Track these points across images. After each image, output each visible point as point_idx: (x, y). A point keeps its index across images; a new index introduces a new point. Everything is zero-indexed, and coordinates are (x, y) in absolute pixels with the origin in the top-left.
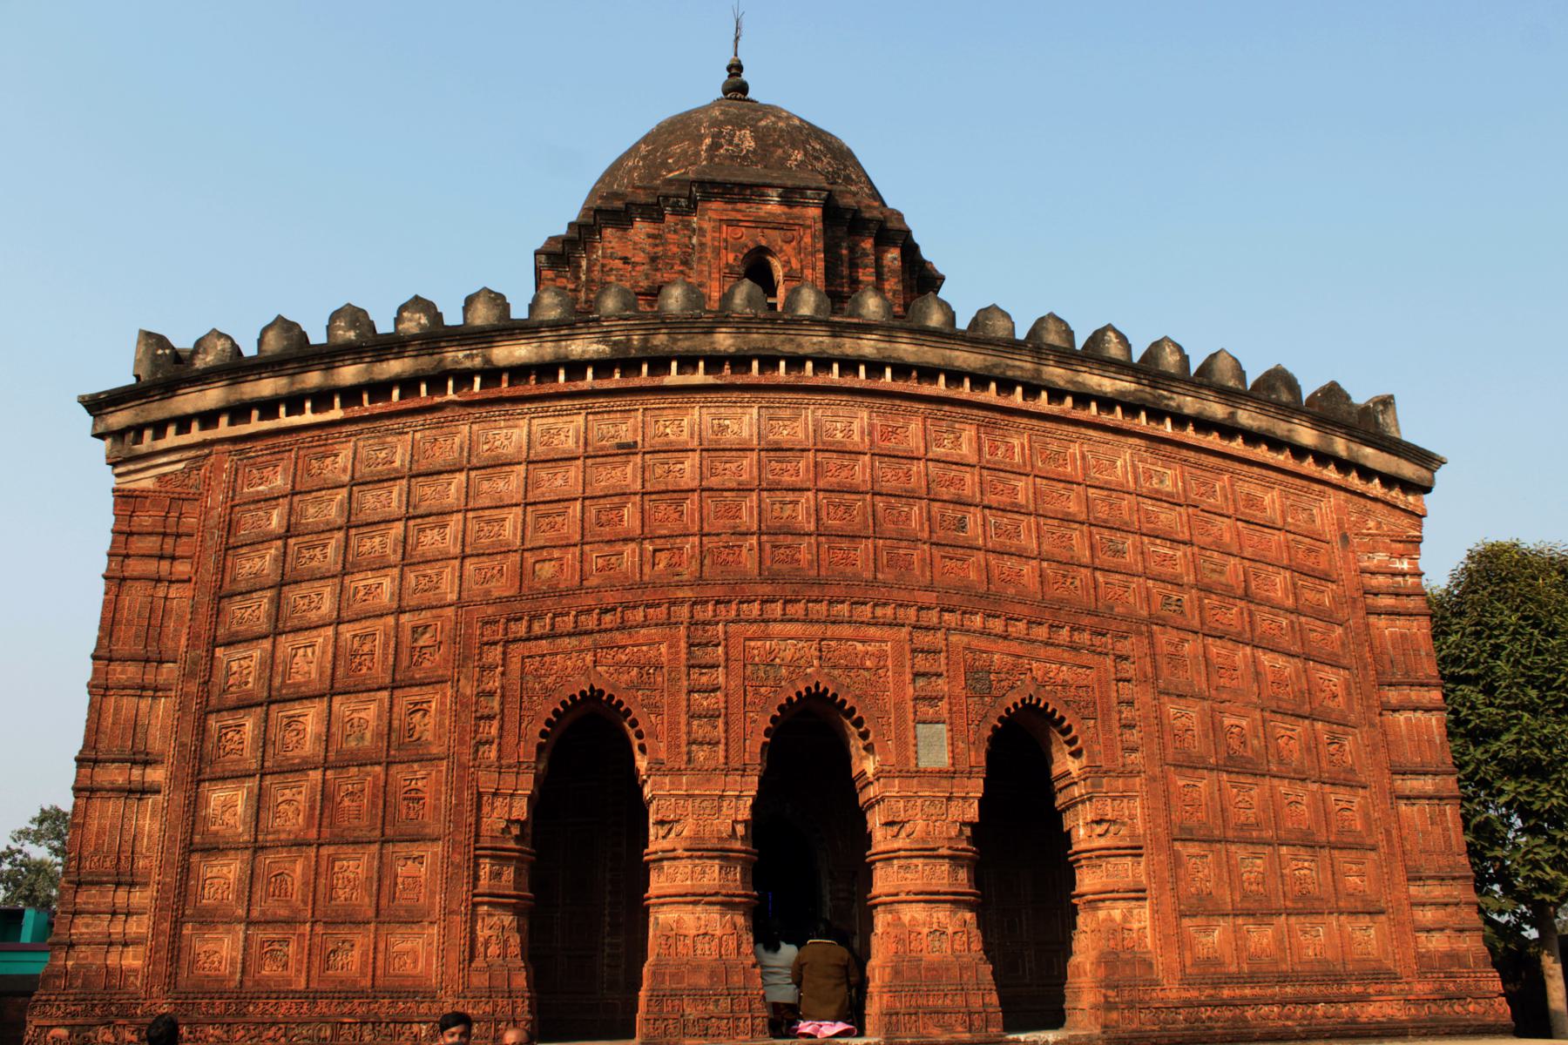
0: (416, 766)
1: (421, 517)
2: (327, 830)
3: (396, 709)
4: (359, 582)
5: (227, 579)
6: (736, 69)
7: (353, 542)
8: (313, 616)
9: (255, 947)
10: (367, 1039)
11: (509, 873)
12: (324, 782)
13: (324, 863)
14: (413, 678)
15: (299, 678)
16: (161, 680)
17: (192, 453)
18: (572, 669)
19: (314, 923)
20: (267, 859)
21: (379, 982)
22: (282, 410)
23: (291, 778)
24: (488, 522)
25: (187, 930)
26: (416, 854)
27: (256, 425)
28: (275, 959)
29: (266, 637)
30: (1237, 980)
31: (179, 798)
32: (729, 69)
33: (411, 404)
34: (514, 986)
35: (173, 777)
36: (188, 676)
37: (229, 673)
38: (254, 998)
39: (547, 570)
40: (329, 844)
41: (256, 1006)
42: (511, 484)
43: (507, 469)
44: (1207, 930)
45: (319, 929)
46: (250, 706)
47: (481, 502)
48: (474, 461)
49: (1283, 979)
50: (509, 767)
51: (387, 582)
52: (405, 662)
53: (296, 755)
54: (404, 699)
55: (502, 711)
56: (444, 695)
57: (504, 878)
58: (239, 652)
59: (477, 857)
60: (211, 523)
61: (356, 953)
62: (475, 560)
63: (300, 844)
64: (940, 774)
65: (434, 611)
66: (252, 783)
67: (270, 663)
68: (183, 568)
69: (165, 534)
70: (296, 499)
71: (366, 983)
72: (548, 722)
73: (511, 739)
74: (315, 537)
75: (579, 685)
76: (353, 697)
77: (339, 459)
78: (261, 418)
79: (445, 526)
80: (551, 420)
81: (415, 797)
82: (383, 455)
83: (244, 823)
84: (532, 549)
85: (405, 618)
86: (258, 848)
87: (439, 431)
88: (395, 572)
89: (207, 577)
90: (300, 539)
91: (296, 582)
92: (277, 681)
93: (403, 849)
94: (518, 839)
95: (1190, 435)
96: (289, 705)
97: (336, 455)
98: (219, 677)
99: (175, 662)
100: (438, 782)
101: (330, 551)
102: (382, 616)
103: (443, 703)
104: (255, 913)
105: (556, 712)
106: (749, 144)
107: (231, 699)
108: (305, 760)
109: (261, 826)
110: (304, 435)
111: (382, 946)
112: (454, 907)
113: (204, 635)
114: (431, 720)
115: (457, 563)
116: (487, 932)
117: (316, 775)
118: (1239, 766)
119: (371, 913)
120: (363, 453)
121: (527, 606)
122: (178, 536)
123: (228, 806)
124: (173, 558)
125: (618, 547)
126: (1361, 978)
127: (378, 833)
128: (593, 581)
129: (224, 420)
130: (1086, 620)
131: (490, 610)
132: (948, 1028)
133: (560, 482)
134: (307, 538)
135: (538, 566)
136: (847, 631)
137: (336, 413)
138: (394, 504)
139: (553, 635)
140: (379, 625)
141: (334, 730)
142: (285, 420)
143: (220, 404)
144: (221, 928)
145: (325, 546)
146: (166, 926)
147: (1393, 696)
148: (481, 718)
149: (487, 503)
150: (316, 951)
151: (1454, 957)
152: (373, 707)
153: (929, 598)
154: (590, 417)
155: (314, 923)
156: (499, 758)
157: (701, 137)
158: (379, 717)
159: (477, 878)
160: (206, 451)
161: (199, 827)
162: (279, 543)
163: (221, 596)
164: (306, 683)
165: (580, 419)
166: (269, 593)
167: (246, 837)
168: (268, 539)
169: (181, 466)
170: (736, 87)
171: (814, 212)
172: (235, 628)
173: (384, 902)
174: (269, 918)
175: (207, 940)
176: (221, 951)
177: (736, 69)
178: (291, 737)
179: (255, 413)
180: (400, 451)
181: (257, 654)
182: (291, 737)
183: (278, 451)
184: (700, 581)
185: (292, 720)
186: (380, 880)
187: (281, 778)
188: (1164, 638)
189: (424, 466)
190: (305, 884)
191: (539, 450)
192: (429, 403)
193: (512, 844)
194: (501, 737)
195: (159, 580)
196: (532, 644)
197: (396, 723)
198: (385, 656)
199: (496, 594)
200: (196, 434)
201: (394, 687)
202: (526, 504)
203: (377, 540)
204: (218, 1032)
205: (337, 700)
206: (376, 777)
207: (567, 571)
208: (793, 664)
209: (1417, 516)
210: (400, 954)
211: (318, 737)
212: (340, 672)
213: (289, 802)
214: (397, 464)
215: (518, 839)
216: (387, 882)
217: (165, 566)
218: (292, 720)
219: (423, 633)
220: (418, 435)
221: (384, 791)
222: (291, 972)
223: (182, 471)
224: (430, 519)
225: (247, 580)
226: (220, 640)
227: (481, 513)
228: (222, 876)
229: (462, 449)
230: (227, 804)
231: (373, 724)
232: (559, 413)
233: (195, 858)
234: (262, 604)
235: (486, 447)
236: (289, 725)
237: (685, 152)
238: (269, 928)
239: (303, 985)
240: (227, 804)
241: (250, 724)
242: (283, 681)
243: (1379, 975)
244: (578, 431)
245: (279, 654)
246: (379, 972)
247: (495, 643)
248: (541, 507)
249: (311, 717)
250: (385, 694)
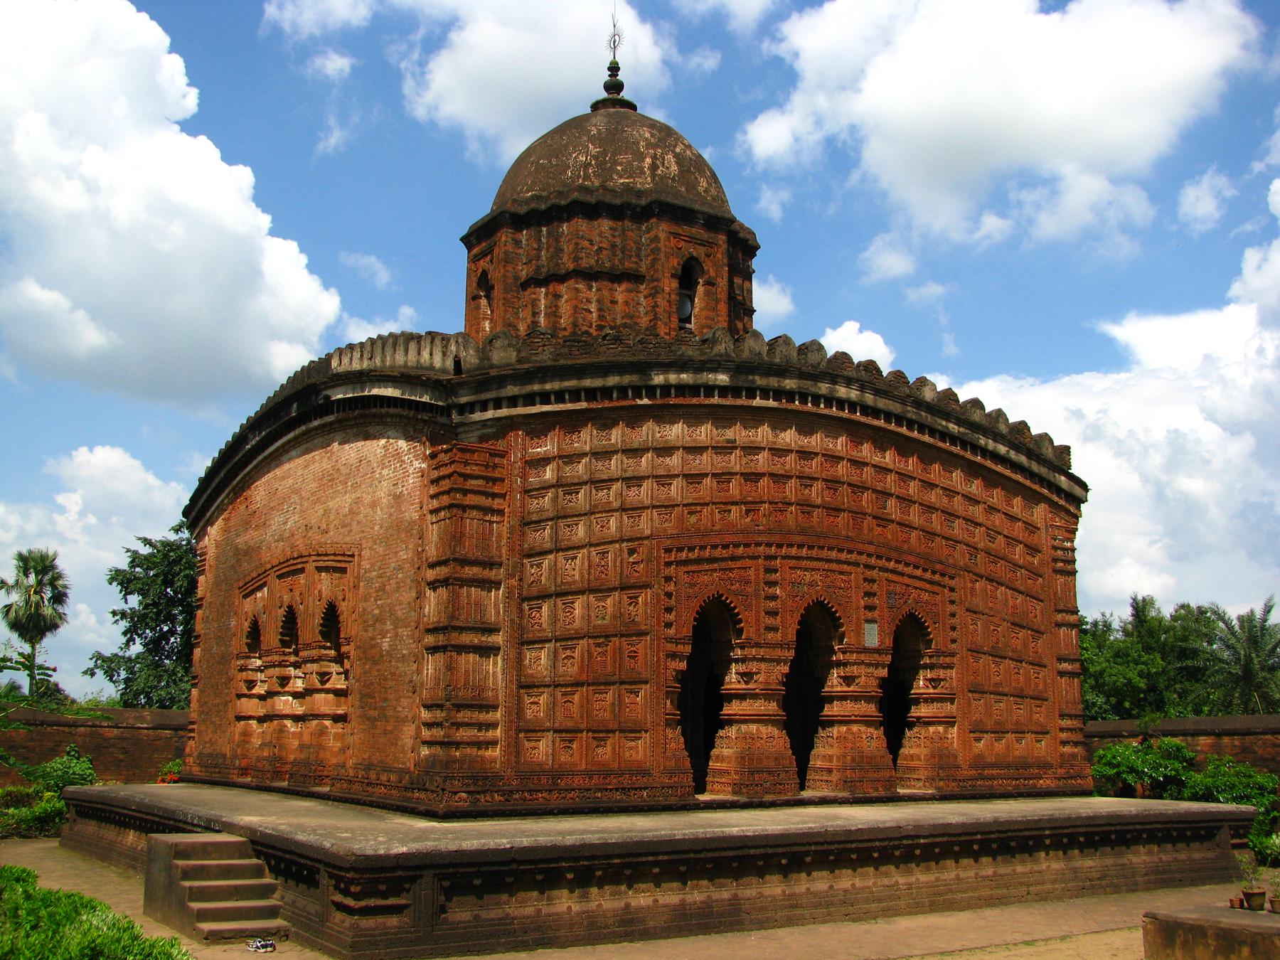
6: (614, 69)
18: (710, 582)
30: (992, 766)
32: (609, 69)
42: (675, 461)
44: (978, 740)
49: (1008, 767)
51: (613, 523)
64: (875, 651)
67: (554, 568)
75: (712, 591)
78: (542, 403)
85: (625, 544)
95: (989, 464)
106: (674, 168)
107: (534, 591)
108: (576, 630)
118: (998, 655)
125: (729, 507)
126: (1039, 767)
128: (718, 527)
130: (938, 567)
131: (668, 542)
132: (877, 789)
136: (834, 566)
140: (611, 548)
146: (513, 733)
147: (1059, 617)
151: (1073, 756)
153: (871, 549)
157: (641, 157)
164: (575, 582)
168: (546, 487)
170: (614, 86)
171: (722, 238)
176: (542, 749)
177: (614, 69)
179: (538, 399)
184: (769, 532)
188: (968, 576)
198: (615, 566)
208: (811, 584)
209: (1076, 517)
211: (583, 617)
231: (610, 610)
237: (630, 163)
243: (1046, 766)
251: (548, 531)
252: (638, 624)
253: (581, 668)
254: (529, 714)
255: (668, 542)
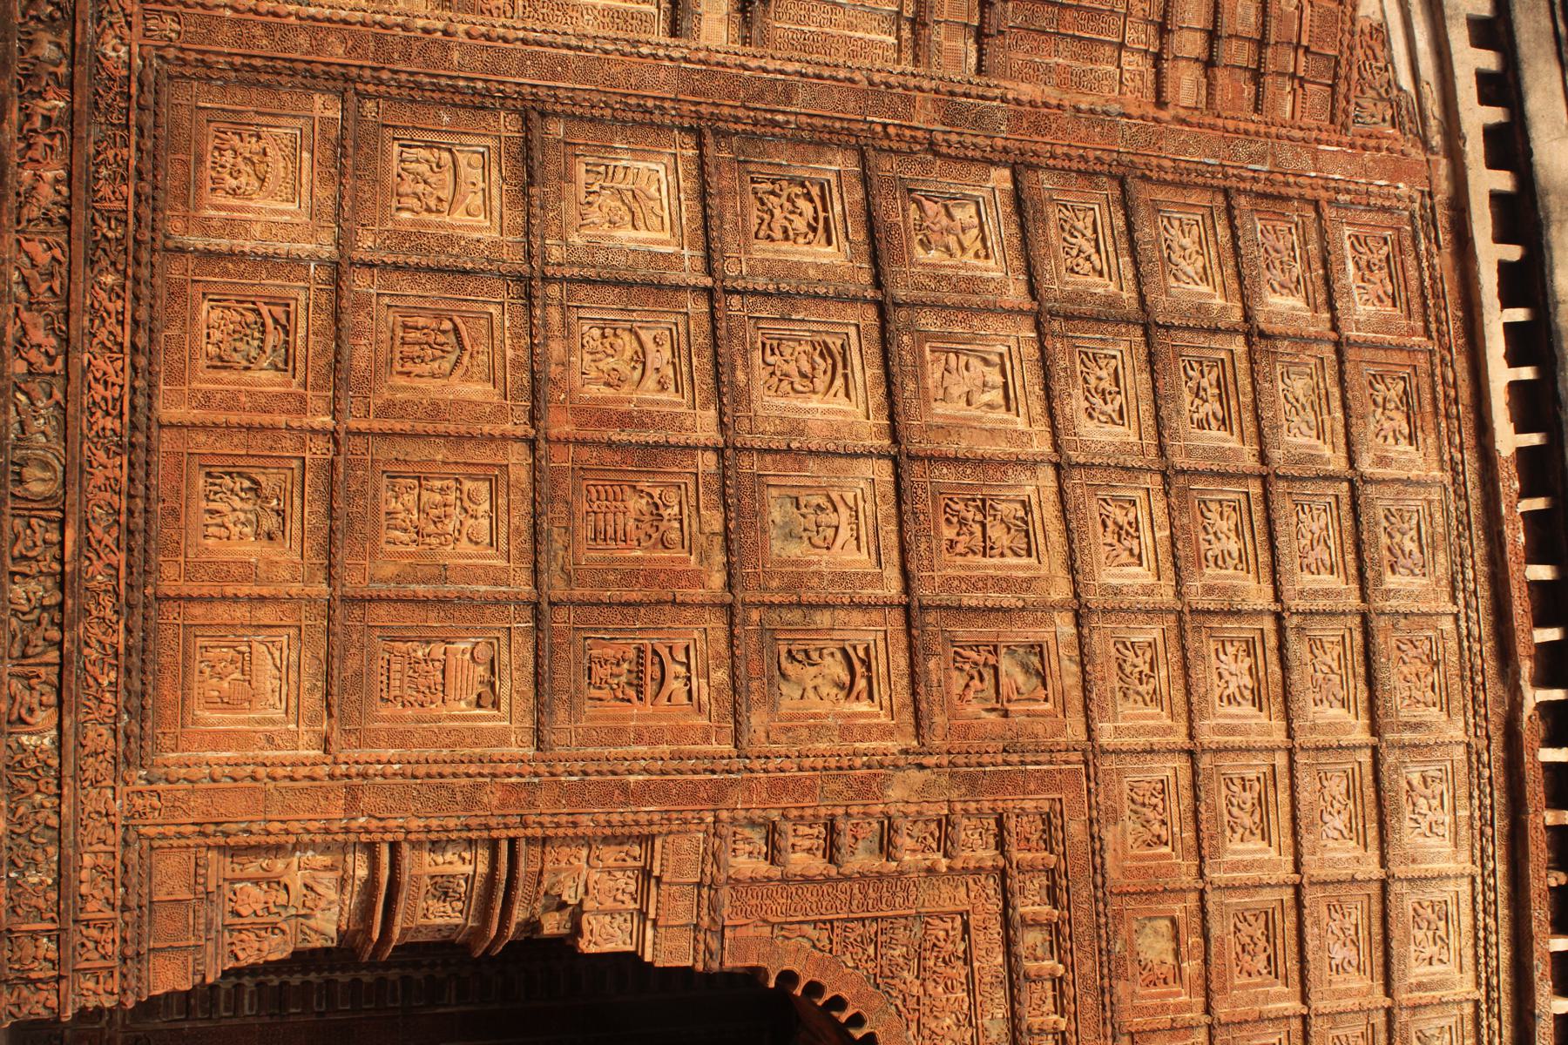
0: (720, 675)
1: (1282, 647)
2: (564, 460)
3: (857, 617)
4: (1145, 504)
5: (1161, 195)
7: (1232, 492)
8: (1074, 404)
9: (273, 284)
10: (18, 591)
11: (445, 916)
12: (689, 449)
13: (484, 455)
14: (929, 653)
15: (934, 373)
16: (939, 35)
17: (1433, 107)
19: (333, 435)
20: (497, 308)
21: (171, 612)
22: (1519, 315)
23: (701, 363)
24: (1261, 801)
25: (325, 107)
26: (504, 691)
27: (1491, 255)
28: (239, 334)
29: (1033, 291)
31: (660, 85)
33: (1520, 607)
34: (157, 962)
35: (711, 67)
36: (950, 104)
37: (949, 202)
38: (136, 287)
39: (1154, 946)
40: (535, 468)
41: (115, 293)
42: (1340, 851)
43: (1372, 833)
45: (318, 450)
46: (875, 259)
47: (1305, 780)
48: (1390, 759)
50: (713, 908)
51: (1141, 575)
52: (962, 632)
53: (755, 374)
54: (876, 635)
55: (848, 878)
56: (887, 733)
57: (436, 906)
58: (1000, 226)
59: (493, 845)
60: (1286, 153)
61: (251, 549)
62: (1185, 780)
63: (537, 391)
65: (1076, 694)
66: (690, 271)
67: (971, 303)
68: (1186, 84)
69: (1262, 43)
70: (1328, 352)
71: (171, 579)
72: (814, 988)
73: (777, 907)
74: (1246, 399)
76: (887, 508)
77: (1404, 445)
78: (1504, 267)
79: (1257, 702)
80: (1466, 921)
81: (645, 675)
82: (1410, 546)
83: (592, 247)
84: (1203, 909)
85: (1064, 626)
86: (527, 287)
87: (1454, 670)
88: (1166, 595)
89: (1169, 147)
90: (1242, 365)
91: (1151, 359)
92: (929, 322)
93: (517, 657)
94: (533, 925)
96: (873, 353)
97: (1411, 438)
98: (942, 178)
99: (980, 70)
100: (680, 734)
101: (1215, 436)
102: (1072, 569)
103: (867, 732)
104: (362, 283)
105: (838, 1003)
107: (893, 210)
108: (742, 396)
109: (583, 292)
110: (1461, 364)
111: (266, 615)
112: (366, 801)
113: (1041, 144)
114: (830, 705)
115: (1181, 739)
116: (296, 880)
117: (704, 425)
119: (353, 583)
120: (1415, 501)
121: (1082, 914)
122: (1257, 76)
123: (634, 207)
124: (1209, 64)
127: (559, 591)
129: (1503, 181)
131: (1076, 828)
133: (1339, 954)
134: (1244, 381)
135: (1164, 925)
137: (1508, 440)
138: (1307, 580)
139: (1014, 979)
140: (1052, 564)
141: (812, 465)
142: (1497, 319)
143: (1541, 174)
144: (325, 193)
145: (1224, 423)
146: (337, 52)
148: (831, 827)
149: (1304, 796)
150: (259, 444)
152: (859, 560)
154: (1468, 1009)
155: (333, 435)
156: (734, 882)
158: (841, 577)
159: (436, 846)
160: (1436, 140)
161: (583, 135)
162: (1236, 316)
163: (1126, 184)
165: (1465, 987)
166: (1128, 295)
167: (556, 254)
169: (1405, 81)
172: (1053, 214)
173: (382, 614)
174: (348, 320)
175: (294, 157)
176: (263, 195)
178: (796, 358)
179: (1513, 253)
180: (1418, 583)
181: (993, 269)
182: (796, 358)
183: (1426, 303)
185: (837, 360)
186: (441, 601)
187: (701, 340)
189: (1385, 642)
190: (435, 411)
191: (1406, 900)
192: (1521, 650)
193: (519, 914)
194: (785, 880)
195: (1163, 30)
196: (996, 929)
197: (823, 619)
199: (1109, 835)
200: (1477, 117)
201: (910, 612)
202: (1298, 889)
203: (1233, 546)
204: (46, 191)
205: (883, 471)
206: (697, 579)
207: (1149, 996)
210: (245, 663)
211: (797, 428)
212: (947, 476)
213: (640, 358)
214: (1391, 581)
215: (533, 925)
216: (433, 619)
217: (1190, 43)
218: (837, 360)
219: (1026, 668)
220: (1447, 624)
221: (662, 599)
222: (204, 381)
223: (1392, 84)
224: (1275, 668)
225: (1156, 242)
226: (1029, 178)
227: (1284, 782)
228: (457, 193)
229: (1415, 727)
230: (635, 205)
231: (823, 560)
232: (1480, 939)
233: (508, 125)
234: (1096, 276)
235: (1416, 779)
236: (826, 352)
238: (322, 320)
239: (169, 411)
240: (635, 205)
241: (832, 257)
242: (928, 337)
244: (1441, 984)
245: (994, 324)
246: (198, 610)
247: (1001, 845)
248: (1291, 918)
249: (843, 409)
250: (892, 588)
251: (1103, 287)
252: (771, 700)
253: (602, 415)
254: (410, 163)
255: (1076, 828)
